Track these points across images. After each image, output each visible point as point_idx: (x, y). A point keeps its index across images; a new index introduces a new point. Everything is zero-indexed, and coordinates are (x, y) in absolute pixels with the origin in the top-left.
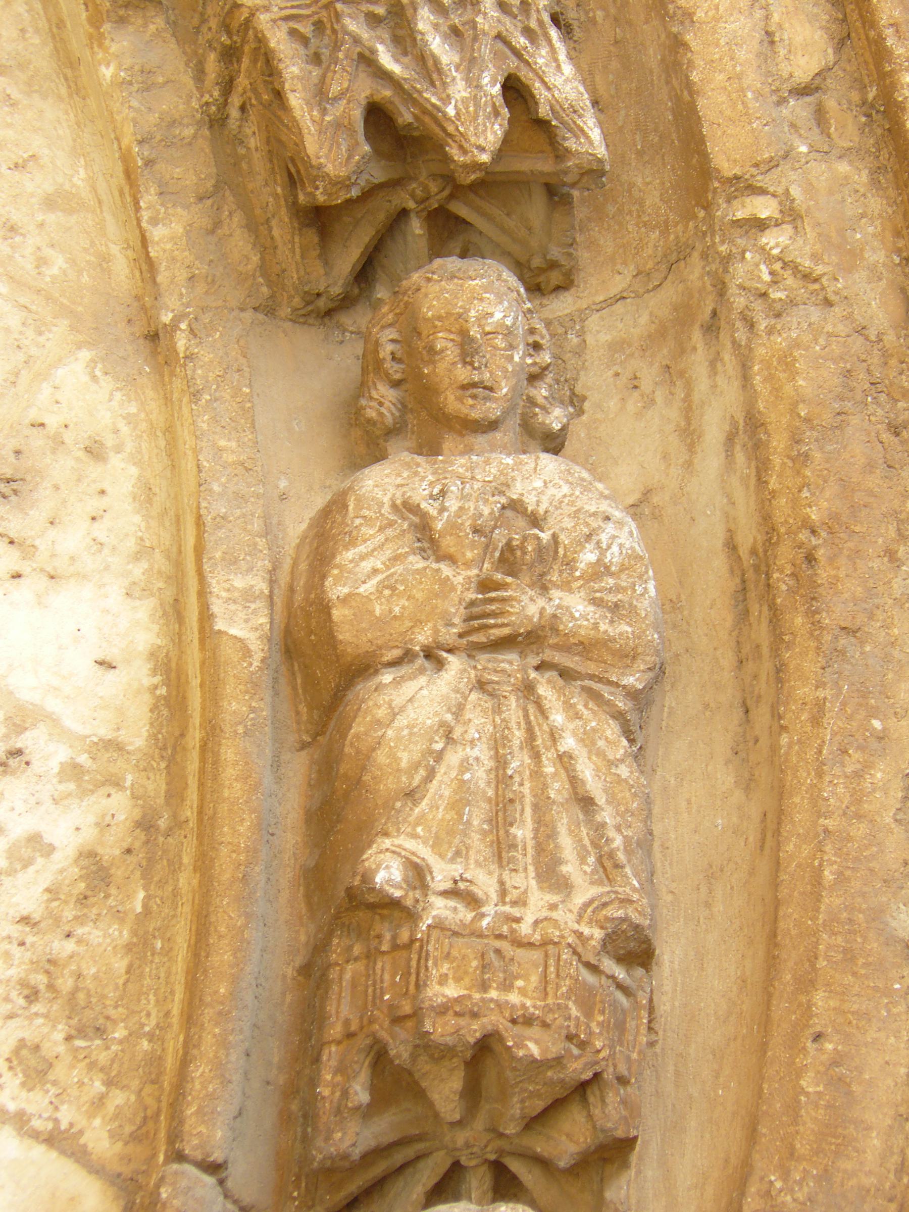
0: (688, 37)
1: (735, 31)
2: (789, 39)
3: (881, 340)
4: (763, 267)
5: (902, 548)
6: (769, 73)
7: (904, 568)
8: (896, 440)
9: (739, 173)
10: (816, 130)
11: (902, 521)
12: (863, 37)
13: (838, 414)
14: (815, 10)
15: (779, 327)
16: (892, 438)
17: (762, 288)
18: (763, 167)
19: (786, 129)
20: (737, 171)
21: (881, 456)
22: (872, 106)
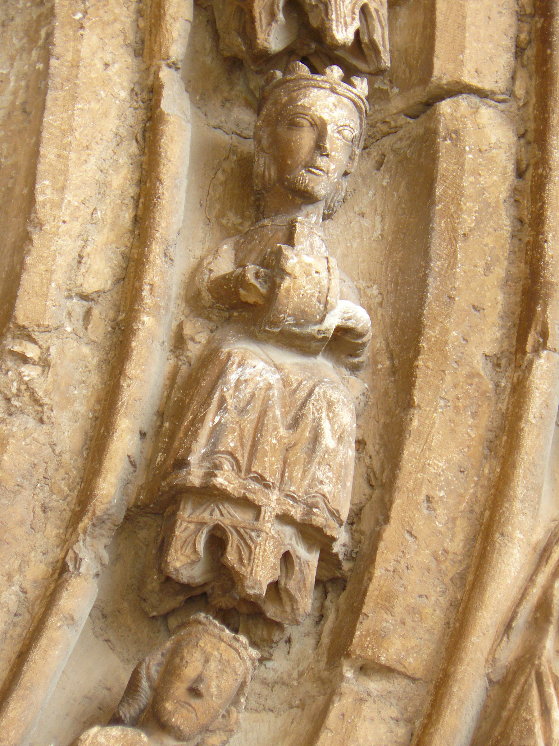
0: (35, 237)
1: (62, 246)
2: (90, 265)
3: (61, 456)
4: (15, 384)
5: (17, 576)
6: (69, 278)
7: (13, 588)
8: (43, 515)
9: (26, 326)
10: (81, 322)
11: (25, 562)
12: (131, 283)
13: (18, 485)
14: (112, 255)
15: (8, 421)
16: (41, 513)
17: (9, 395)
18: (42, 329)
19: (64, 314)
20: (26, 324)
21: (30, 520)
22: (118, 324)
